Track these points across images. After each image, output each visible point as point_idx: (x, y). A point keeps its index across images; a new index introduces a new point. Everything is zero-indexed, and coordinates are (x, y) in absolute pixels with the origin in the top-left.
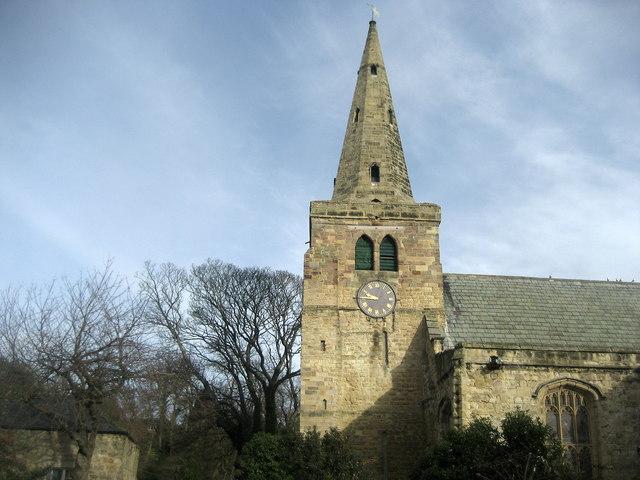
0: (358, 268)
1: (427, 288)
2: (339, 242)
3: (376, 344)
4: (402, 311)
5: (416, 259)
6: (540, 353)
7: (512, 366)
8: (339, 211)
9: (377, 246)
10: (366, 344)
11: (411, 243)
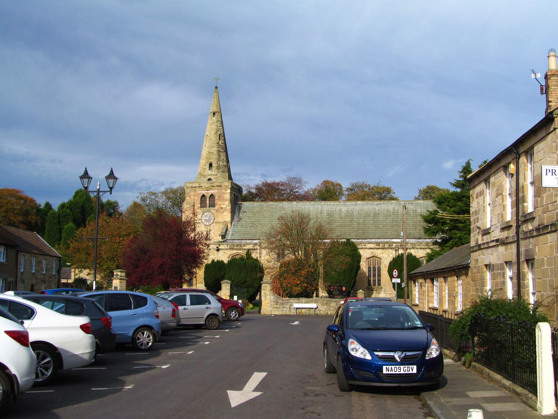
1: (224, 214)
4: (216, 223)
5: (222, 203)
7: (223, 249)
8: (194, 186)
11: (219, 197)
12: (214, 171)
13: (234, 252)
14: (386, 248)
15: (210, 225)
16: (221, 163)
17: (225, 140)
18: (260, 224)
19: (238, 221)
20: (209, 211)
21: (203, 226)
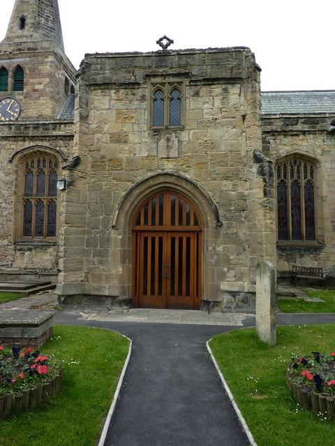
1: (41, 101)
5: (39, 80)
9: (10, 73)
11: (33, 70)
13: (27, 144)
16: (43, 21)
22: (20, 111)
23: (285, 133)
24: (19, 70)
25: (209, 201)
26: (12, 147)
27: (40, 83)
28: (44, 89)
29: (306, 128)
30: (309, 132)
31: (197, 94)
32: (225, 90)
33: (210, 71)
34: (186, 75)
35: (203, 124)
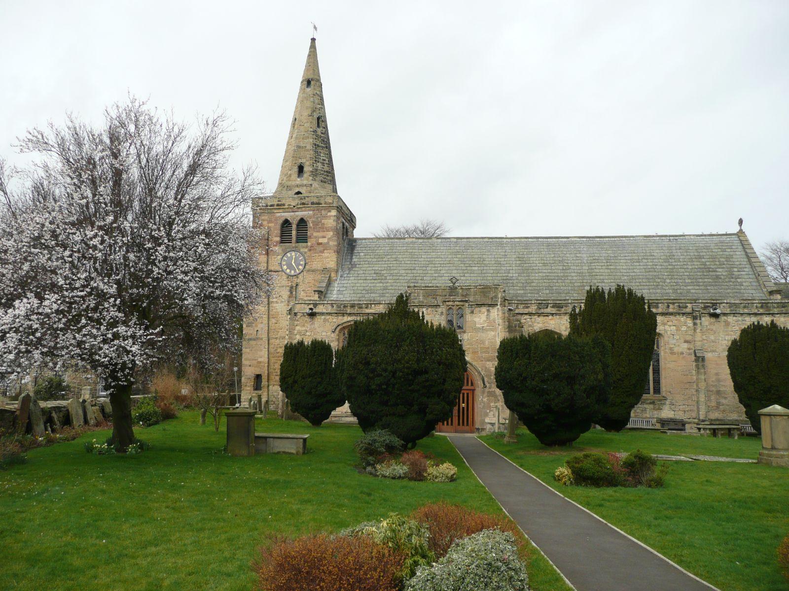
0: (282, 242)
1: (326, 254)
2: (270, 225)
3: (291, 293)
4: (308, 271)
6: (339, 307)
7: (323, 314)
9: (294, 226)
10: (285, 293)
12: (306, 179)
13: (346, 319)
14: (671, 314)
15: (296, 276)
16: (319, 165)
17: (326, 127)
18: (391, 275)
19: (350, 269)
20: (296, 250)
21: (285, 277)
22: (305, 264)
23: (539, 315)
24: (302, 222)
25: (479, 373)
26: (334, 320)
27: (324, 237)
28: (328, 243)
29: (554, 311)
30: (556, 314)
31: (472, 312)
32: (488, 311)
33: (479, 299)
34: (466, 301)
35: (477, 330)
